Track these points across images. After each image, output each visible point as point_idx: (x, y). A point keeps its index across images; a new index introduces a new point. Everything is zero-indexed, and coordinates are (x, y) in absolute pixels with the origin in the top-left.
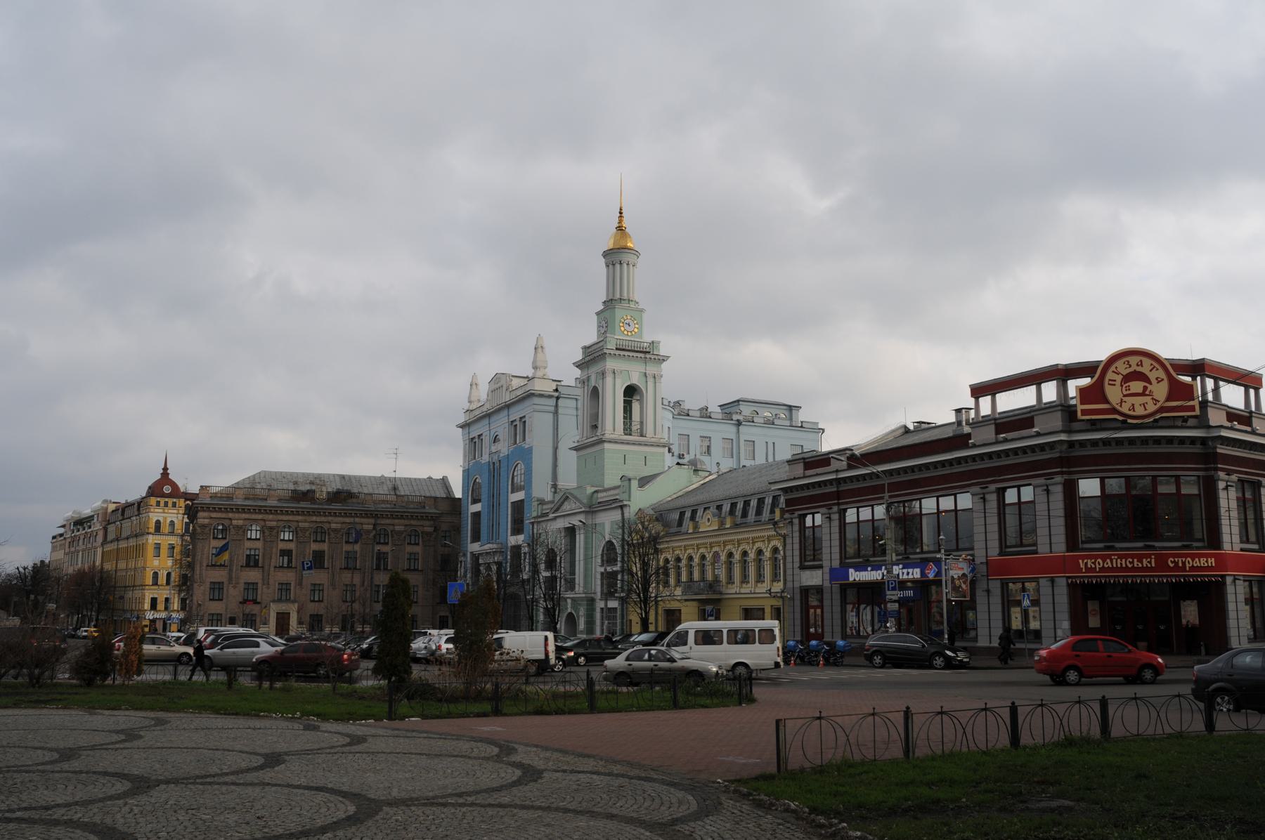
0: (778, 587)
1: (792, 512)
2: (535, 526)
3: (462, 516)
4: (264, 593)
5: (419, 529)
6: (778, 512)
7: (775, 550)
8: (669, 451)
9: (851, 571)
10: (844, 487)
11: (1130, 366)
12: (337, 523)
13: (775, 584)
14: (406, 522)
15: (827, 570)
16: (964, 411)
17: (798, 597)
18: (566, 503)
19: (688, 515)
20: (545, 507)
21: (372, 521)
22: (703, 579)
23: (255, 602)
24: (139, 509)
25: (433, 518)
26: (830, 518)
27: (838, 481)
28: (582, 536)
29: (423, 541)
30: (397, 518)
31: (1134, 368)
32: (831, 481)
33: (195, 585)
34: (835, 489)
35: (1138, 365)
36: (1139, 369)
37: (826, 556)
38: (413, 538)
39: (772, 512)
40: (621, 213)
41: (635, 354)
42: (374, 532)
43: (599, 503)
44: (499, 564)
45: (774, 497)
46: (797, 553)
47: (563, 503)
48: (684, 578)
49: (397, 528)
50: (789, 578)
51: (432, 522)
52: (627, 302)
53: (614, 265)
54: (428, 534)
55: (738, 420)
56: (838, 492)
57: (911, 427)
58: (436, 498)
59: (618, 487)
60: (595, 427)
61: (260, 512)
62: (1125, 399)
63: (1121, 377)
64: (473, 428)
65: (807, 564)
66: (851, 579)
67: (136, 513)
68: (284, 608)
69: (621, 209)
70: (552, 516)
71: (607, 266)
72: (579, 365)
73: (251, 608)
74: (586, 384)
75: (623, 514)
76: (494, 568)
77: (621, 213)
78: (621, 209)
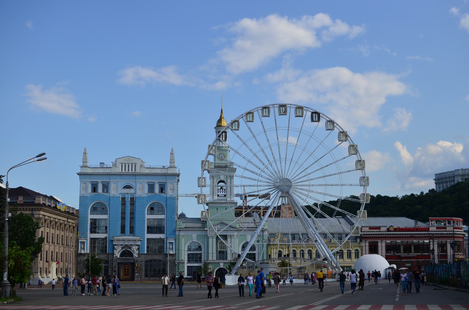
21: (66, 219)
40: (222, 111)
44: (139, 245)
52: (225, 147)
69: (222, 110)
77: (222, 111)
78: (222, 110)
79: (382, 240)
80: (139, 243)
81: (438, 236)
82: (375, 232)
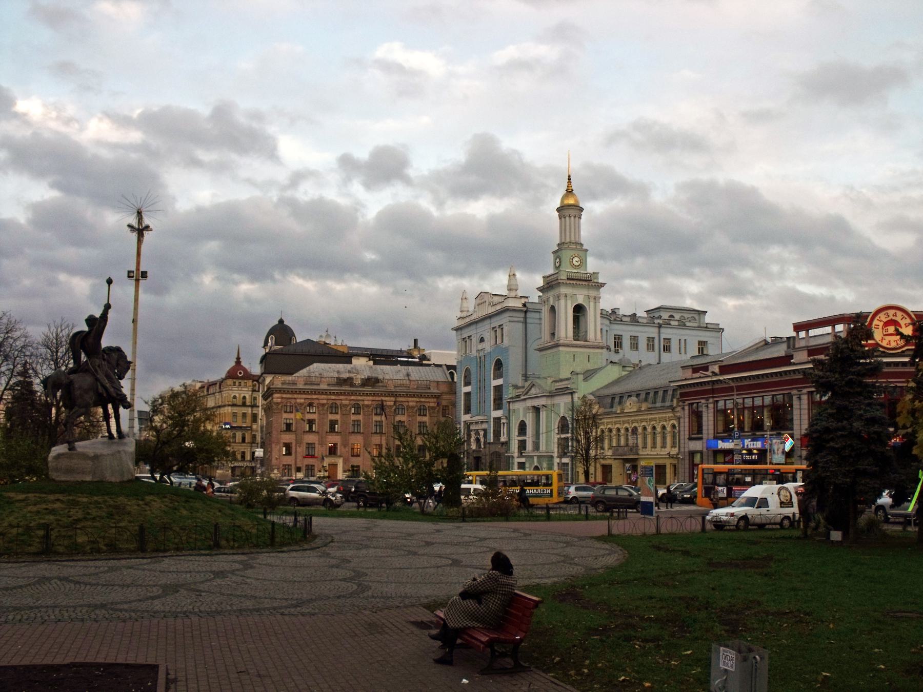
0: (674, 451)
1: (684, 402)
2: (511, 404)
3: (457, 395)
4: (319, 450)
5: (427, 405)
6: (675, 401)
7: (674, 426)
8: (608, 349)
9: (720, 442)
10: (716, 386)
11: (889, 316)
12: (368, 401)
13: (673, 449)
14: (417, 399)
15: (705, 441)
16: (792, 339)
17: (687, 458)
18: (533, 389)
19: (617, 400)
20: (519, 391)
21: (393, 399)
22: (627, 445)
23: (313, 456)
24: (220, 388)
25: (438, 397)
26: (707, 406)
27: (713, 382)
28: (544, 412)
29: (429, 413)
30: (411, 396)
31: (891, 317)
32: (708, 382)
33: (273, 445)
34: (710, 388)
35: (893, 316)
36: (894, 318)
37: (704, 432)
38: (422, 411)
39: (672, 401)
40: (569, 179)
41: (581, 283)
42: (395, 407)
43: (556, 389)
44: (485, 430)
45: (674, 390)
46: (687, 429)
47: (531, 389)
48: (614, 444)
49: (411, 404)
50: (682, 445)
51: (435, 400)
53: (565, 218)
54: (433, 408)
55: (659, 323)
56: (713, 389)
57: (769, 340)
58: (438, 382)
59: (569, 379)
60: (553, 334)
61: (315, 394)
62: (884, 337)
63: (882, 323)
64: (463, 331)
65: (693, 436)
66: (719, 447)
67: (218, 390)
68: (333, 461)
69: (569, 176)
70: (522, 397)
71: (560, 218)
72: (541, 289)
73: (310, 461)
74: (546, 303)
75: (572, 398)
76: (482, 433)
77: (569, 179)
78: (569, 176)
79: (707, 399)
80: (484, 426)
81: (779, 379)
82: (700, 378)
